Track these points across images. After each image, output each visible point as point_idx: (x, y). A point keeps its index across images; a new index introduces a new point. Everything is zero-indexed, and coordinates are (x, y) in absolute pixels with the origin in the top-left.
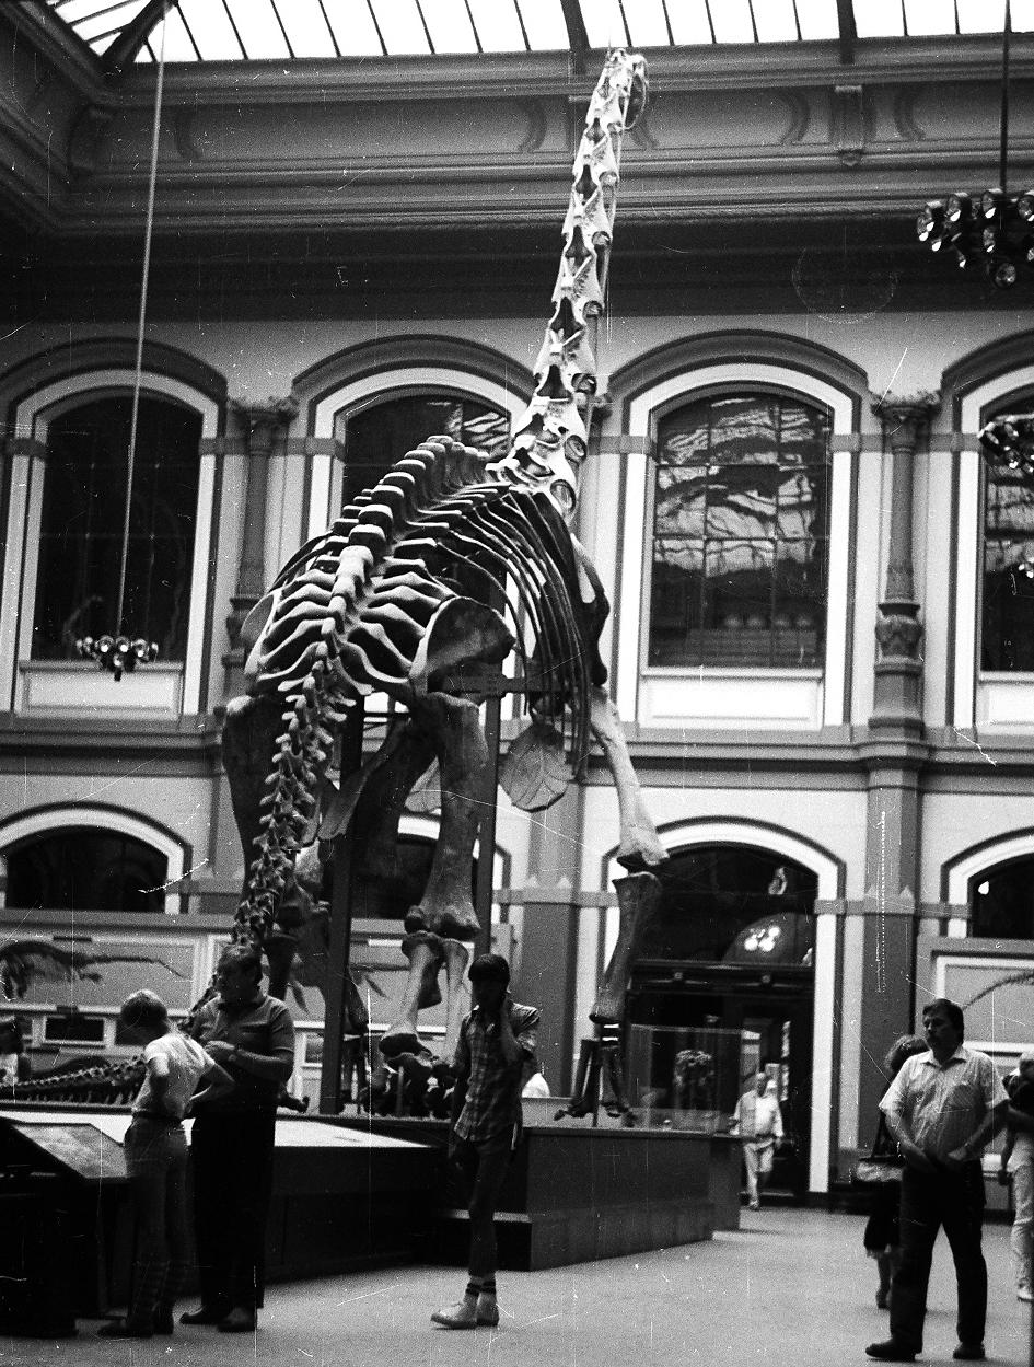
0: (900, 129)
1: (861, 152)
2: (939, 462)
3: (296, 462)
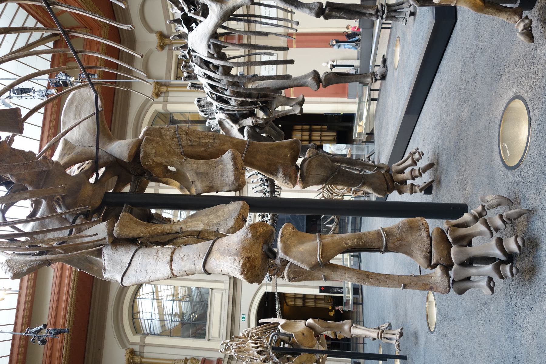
3: (146, 349)
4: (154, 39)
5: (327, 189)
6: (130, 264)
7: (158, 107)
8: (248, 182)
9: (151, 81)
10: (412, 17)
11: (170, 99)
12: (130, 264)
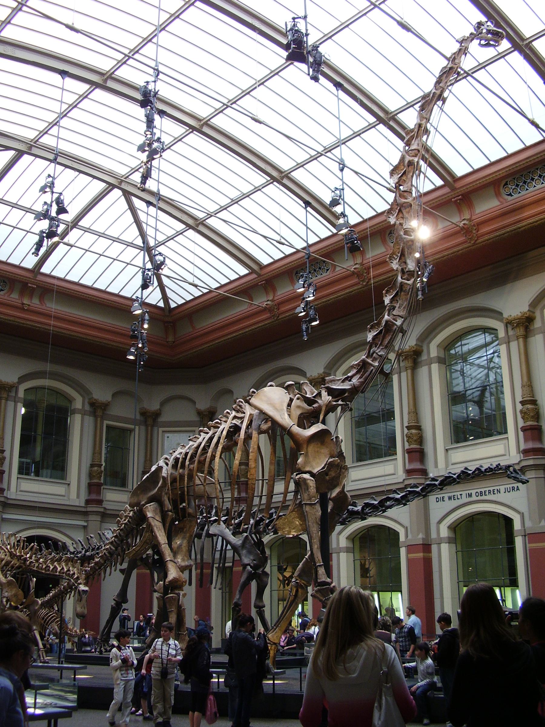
0: (40, 301)
1: (29, 305)
4: (154, 406)
5: (47, 614)
6: (157, 520)
7: (78, 403)
9: (110, 399)
11: (87, 418)
12: (157, 520)
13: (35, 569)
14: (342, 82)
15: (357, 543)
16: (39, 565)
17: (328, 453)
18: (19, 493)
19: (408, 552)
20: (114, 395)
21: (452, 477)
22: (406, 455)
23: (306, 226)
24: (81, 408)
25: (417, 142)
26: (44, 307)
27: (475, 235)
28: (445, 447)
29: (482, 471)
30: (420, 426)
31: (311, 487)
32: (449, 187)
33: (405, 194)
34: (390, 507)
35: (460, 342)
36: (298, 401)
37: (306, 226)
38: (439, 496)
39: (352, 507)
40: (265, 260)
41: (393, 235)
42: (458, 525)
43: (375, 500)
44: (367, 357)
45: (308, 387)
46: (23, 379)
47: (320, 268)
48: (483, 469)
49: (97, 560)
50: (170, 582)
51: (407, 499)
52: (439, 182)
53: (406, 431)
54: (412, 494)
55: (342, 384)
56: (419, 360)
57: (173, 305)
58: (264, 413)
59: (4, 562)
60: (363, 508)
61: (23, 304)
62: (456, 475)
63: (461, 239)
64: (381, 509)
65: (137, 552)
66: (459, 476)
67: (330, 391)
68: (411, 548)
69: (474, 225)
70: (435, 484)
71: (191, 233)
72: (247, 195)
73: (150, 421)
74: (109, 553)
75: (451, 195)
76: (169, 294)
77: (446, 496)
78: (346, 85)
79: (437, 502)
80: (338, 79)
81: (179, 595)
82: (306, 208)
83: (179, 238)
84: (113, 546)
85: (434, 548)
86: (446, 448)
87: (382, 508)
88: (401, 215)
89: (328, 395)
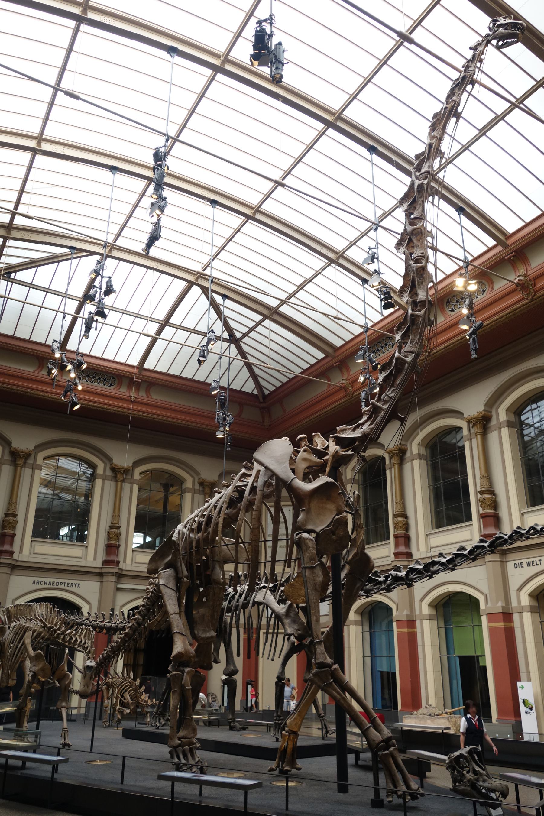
1: (136, 398)
2: (127, 486)
5: (122, 682)
6: (170, 588)
8: (102, 582)
9: (216, 478)
10: (275, 740)
11: (196, 495)
12: (170, 588)
13: (60, 641)
14: (376, 145)
15: (366, 616)
16: (64, 637)
17: (335, 509)
18: (134, 564)
19: (490, 621)
20: (221, 475)
21: (503, 537)
22: (481, 520)
23: (364, 301)
24: (191, 487)
25: (427, 164)
26: (150, 399)
27: (532, 290)
28: (520, 511)
29: (537, 531)
30: (494, 491)
31: (310, 547)
32: (501, 246)
33: (416, 221)
34: (437, 572)
35: (530, 406)
36: (305, 453)
37: (364, 301)
38: (517, 562)
39: (396, 572)
40: (338, 343)
41: (451, 303)
42: (541, 592)
43: (420, 565)
44: (377, 401)
45: (319, 439)
46: (137, 463)
47: (386, 345)
48: (539, 528)
49: (127, 630)
50: (174, 657)
51: (454, 563)
52: (491, 242)
53: (479, 496)
54: (460, 558)
55: (352, 432)
56: (489, 425)
57: (267, 392)
58: (271, 471)
59: (35, 634)
60: (407, 574)
61: (131, 397)
62: (508, 536)
63: (519, 296)
64: (426, 574)
65: (159, 622)
66: (511, 537)
67: (339, 441)
68: (491, 617)
69: (530, 280)
70: (484, 547)
71: (267, 323)
72: (310, 280)
73: (207, 491)
74: (137, 623)
75: (504, 253)
76: (263, 383)
77: (525, 562)
78: (380, 148)
79: (515, 568)
80: (371, 143)
81: (183, 672)
82: (363, 285)
83: (259, 329)
84: (141, 616)
85: (516, 617)
86: (522, 512)
87: (427, 573)
88: (411, 244)
89: (336, 445)
